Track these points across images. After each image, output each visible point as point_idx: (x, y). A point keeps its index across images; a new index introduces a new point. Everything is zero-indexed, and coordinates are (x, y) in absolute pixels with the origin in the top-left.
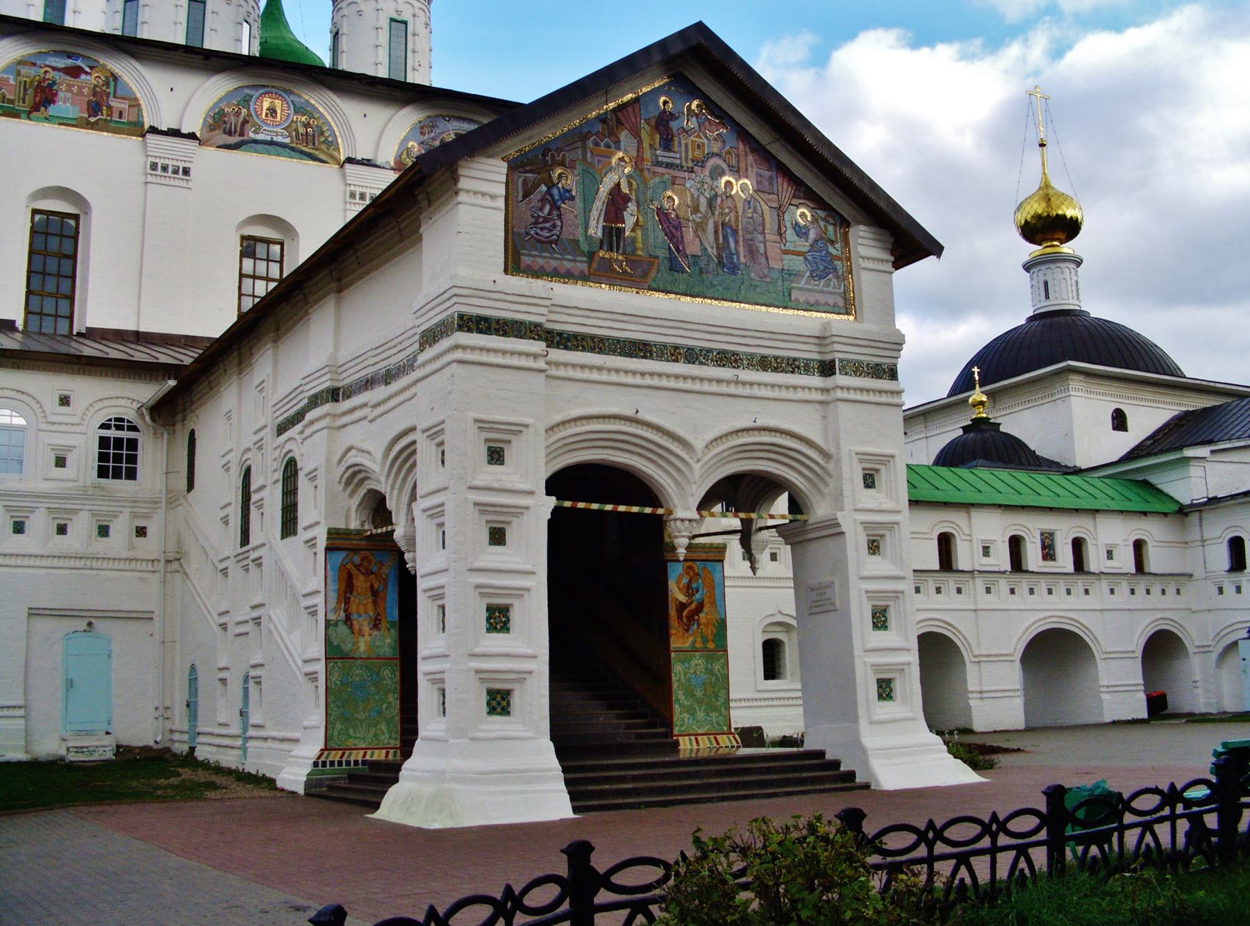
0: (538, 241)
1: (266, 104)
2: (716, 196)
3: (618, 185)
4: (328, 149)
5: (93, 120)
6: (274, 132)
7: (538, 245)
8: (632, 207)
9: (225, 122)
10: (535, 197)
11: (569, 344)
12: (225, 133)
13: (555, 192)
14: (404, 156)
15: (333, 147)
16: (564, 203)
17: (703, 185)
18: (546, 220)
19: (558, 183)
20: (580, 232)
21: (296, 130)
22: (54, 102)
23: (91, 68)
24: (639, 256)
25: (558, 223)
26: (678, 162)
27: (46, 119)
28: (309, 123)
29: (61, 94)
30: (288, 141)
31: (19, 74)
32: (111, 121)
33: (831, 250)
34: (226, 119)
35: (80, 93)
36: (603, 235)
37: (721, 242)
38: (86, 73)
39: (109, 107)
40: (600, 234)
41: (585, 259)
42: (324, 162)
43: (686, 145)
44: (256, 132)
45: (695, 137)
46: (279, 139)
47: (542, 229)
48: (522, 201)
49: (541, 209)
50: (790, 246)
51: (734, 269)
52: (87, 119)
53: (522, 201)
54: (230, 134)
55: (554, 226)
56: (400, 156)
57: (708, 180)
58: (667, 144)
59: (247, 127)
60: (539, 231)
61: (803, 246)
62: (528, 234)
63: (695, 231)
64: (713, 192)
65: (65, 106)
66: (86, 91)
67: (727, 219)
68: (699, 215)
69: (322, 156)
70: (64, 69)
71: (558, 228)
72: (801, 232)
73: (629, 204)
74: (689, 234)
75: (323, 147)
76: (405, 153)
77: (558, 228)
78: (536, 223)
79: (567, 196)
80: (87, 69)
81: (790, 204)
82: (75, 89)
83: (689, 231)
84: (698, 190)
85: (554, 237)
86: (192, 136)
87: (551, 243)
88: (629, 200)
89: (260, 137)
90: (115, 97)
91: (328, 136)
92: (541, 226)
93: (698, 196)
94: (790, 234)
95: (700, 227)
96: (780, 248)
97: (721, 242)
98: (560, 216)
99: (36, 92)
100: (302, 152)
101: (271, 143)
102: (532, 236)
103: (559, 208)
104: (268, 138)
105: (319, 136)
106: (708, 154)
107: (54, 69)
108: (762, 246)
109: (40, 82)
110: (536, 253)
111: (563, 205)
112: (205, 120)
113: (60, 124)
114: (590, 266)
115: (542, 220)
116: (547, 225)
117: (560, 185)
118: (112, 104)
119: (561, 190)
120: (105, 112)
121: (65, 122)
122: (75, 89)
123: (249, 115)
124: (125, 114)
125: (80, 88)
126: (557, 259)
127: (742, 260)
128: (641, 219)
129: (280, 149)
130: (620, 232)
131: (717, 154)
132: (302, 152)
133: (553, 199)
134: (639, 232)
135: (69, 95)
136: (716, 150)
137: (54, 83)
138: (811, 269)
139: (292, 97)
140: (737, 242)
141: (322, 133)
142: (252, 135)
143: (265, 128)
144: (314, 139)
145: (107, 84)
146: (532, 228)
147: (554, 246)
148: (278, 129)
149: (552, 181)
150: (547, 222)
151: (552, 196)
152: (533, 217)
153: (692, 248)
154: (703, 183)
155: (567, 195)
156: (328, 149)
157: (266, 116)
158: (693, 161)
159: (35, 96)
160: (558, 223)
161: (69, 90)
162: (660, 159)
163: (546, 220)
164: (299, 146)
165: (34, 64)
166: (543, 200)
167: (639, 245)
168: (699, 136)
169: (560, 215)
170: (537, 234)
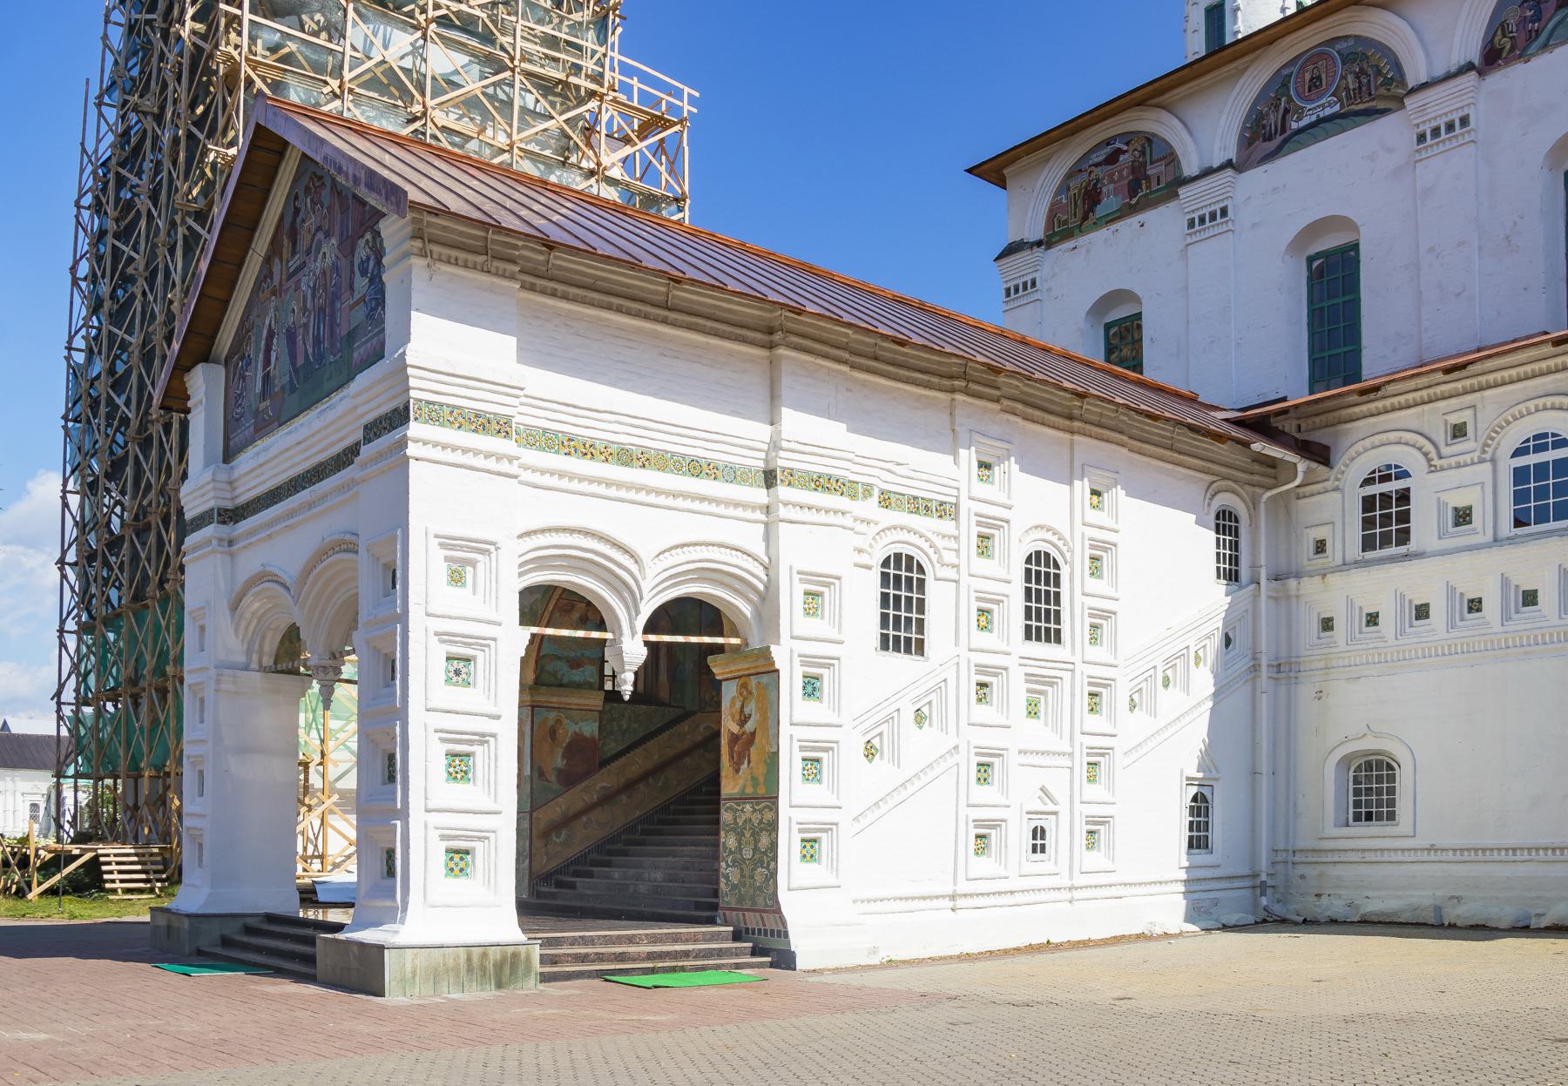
1: (1308, 76)
4: (1389, 90)
5: (1134, 202)
6: (1319, 106)
9: (1264, 127)
12: (1264, 140)
14: (1497, 39)
15: (1395, 84)
21: (1347, 89)
22: (1099, 202)
23: (1127, 144)
27: (1095, 223)
28: (1361, 69)
29: (1104, 190)
30: (1337, 108)
31: (1069, 189)
32: (1151, 193)
34: (1265, 122)
35: (1121, 177)
38: (1124, 152)
39: (1148, 178)
42: (1383, 112)
44: (1299, 119)
46: (1328, 111)
52: (1129, 203)
54: (1268, 138)
56: (1492, 41)
59: (1288, 117)
65: (1109, 203)
66: (1125, 173)
69: (1381, 105)
70: (1104, 160)
75: (1382, 91)
76: (1499, 32)
80: (1125, 148)
82: (1116, 177)
86: (1229, 164)
89: (1302, 124)
90: (1152, 163)
91: (1387, 73)
99: (1084, 200)
100: (1357, 113)
101: (1320, 121)
104: (1314, 118)
105: (1375, 78)
107: (1097, 165)
109: (1086, 188)
112: (1241, 136)
113: (1107, 223)
118: (1149, 173)
120: (1144, 187)
121: (1111, 219)
122: (1116, 177)
123: (1290, 100)
124: (1163, 179)
125: (1120, 172)
129: (1328, 125)
132: (1357, 113)
135: (1111, 187)
137: (1098, 180)
139: (1338, 47)
141: (1379, 72)
142: (1294, 126)
143: (1309, 107)
144: (1369, 88)
145: (1143, 153)
148: (1324, 101)
156: (1389, 90)
157: (1310, 91)
159: (1084, 204)
161: (1112, 181)
164: (1353, 107)
165: (1081, 171)
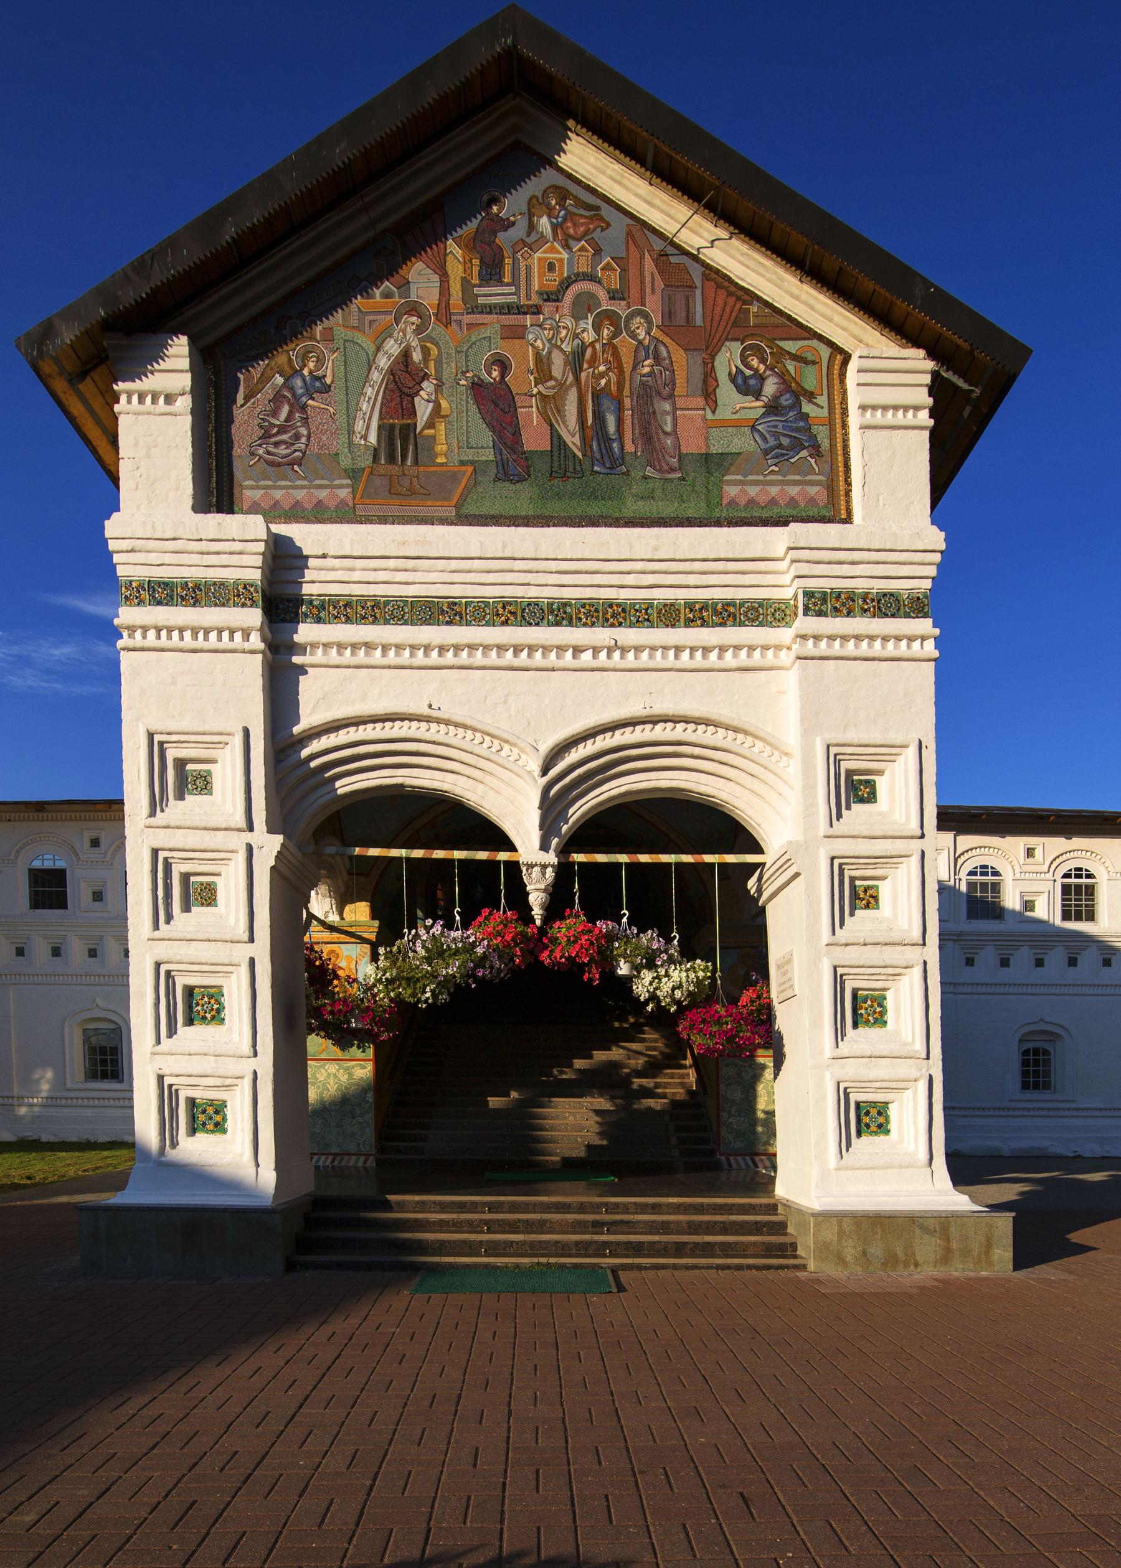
0: (272, 464)
2: (583, 347)
3: (406, 354)
7: (270, 469)
8: (428, 386)
10: (268, 391)
11: (322, 615)
13: (298, 382)
16: (313, 399)
17: (558, 332)
18: (282, 430)
19: (302, 369)
20: (344, 438)
24: (441, 465)
25: (304, 431)
26: (512, 299)
33: (807, 408)
36: (379, 441)
37: (590, 421)
40: (373, 438)
41: (349, 482)
43: (529, 269)
45: (545, 252)
47: (277, 444)
48: (242, 406)
49: (275, 413)
50: (724, 413)
51: (614, 463)
53: (242, 406)
55: (297, 437)
57: (568, 322)
58: (492, 271)
60: (271, 449)
61: (753, 408)
62: (253, 454)
63: (543, 414)
64: (577, 341)
67: (603, 382)
68: (551, 383)
71: (304, 440)
72: (747, 386)
73: (425, 385)
74: (530, 415)
77: (304, 440)
78: (266, 436)
79: (319, 387)
81: (727, 339)
83: (530, 414)
84: (549, 341)
85: (297, 454)
87: (291, 464)
88: (426, 377)
92: (273, 440)
93: (550, 353)
94: (726, 392)
95: (551, 405)
96: (704, 418)
97: (590, 421)
98: (305, 421)
102: (261, 457)
103: (303, 408)
106: (569, 277)
108: (669, 419)
110: (270, 483)
111: (310, 402)
114: (354, 492)
115: (275, 430)
116: (285, 437)
117: (306, 372)
119: (307, 378)
126: (302, 487)
127: (629, 447)
128: (444, 404)
130: (408, 431)
131: (584, 274)
133: (294, 395)
134: (441, 427)
136: (583, 269)
138: (763, 446)
140: (620, 421)
146: (260, 445)
147: (296, 468)
149: (292, 367)
150: (285, 432)
151: (292, 389)
152: (261, 427)
153: (534, 438)
154: (556, 329)
155: (317, 384)
158: (540, 293)
160: (304, 431)
162: (481, 300)
163: (282, 430)
166: (278, 399)
167: (441, 448)
168: (553, 250)
169: (307, 418)
170: (269, 453)
